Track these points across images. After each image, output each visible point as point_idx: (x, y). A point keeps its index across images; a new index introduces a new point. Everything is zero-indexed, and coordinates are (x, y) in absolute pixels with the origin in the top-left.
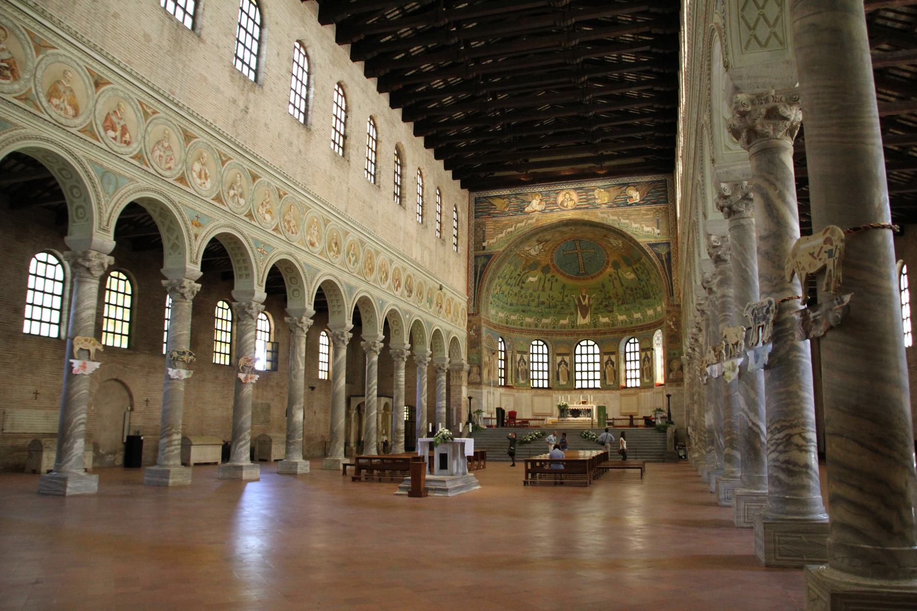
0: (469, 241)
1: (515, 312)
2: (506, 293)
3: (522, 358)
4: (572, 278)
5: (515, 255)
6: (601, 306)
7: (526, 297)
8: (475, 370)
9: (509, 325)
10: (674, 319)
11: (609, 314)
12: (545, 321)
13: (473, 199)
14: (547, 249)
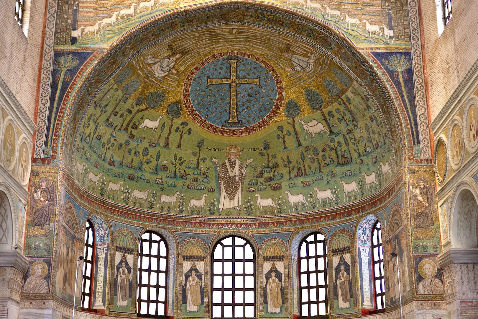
0: (44, 27)
1: (118, 176)
2: (104, 140)
3: (124, 261)
4: (215, 130)
5: (127, 67)
6: (261, 180)
7: (137, 154)
8: (39, 269)
9: (105, 198)
10: (422, 184)
11: (276, 193)
12: (165, 199)
14: (182, 69)
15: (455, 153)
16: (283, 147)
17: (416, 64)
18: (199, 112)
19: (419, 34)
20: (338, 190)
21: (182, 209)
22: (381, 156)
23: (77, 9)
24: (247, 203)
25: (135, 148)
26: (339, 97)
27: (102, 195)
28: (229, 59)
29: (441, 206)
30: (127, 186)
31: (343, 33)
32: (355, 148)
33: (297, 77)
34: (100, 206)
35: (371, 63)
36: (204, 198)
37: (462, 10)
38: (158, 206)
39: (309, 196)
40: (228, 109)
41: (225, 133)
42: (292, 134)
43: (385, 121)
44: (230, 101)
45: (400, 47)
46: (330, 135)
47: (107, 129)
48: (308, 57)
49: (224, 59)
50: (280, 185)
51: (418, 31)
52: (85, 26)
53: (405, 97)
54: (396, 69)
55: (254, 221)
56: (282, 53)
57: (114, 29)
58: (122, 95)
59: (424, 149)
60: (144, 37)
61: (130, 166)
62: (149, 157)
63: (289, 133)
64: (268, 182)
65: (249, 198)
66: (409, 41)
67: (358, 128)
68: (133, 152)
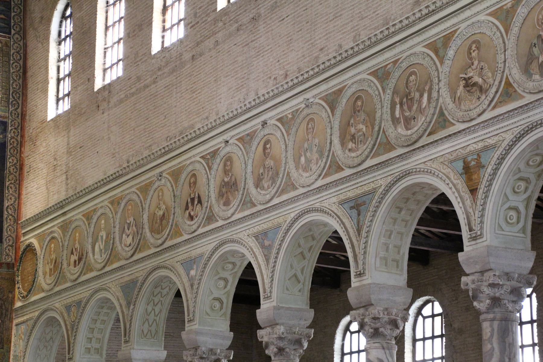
15: (48, 270)
17: (12, 138)
29: (17, 325)
37: (83, 111)
51: (19, 94)
59: (7, 250)
66: (6, 107)
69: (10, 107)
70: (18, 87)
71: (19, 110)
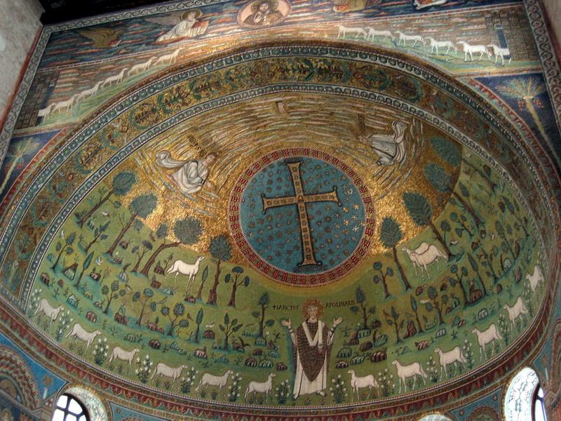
1: (131, 341)
2: (108, 282)
4: (284, 278)
6: (356, 348)
7: (165, 311)
9: (102, 369)
11: (378, 366)
12: (209, 379)
13: (46, 35)
16: (384, 294)
18: (258, 251)
19: (552, 48)
20: (471, 345)
21: (236, 394)
22: (526, 264)
23: (53, 88)
24: (336, 384)
25: (160, 303)
26: (452, 191)
27: (98, 362)
28: (287, 162)
30: (147, 357)
31: (428, 59)
32: (488, 268)
33: (387, 176)
34: (93, 379)
35: (478, 93)
36: (270, 379)
38: (196, 390)
39: (428, 363)
40: (299, 245)
41: (299, 282)
42: (396, 272)
43: (519, 195)
44: (301, 232)
45: (523, 67)
46: (449, 260)
47: (111, 266)
48: (391, 132)
49: (280, 164)
50: (385, 351)
52: (57, 102)
53: (543, 132)
54: (520, 97)
55: (346, 411)
56: (357, 136)
57: (93, 99)
58: (130, 216)
60: (140, 112)
61: (154, 327)
62: (185, 316)
63: (390, 272)
64: (366, 350)
65: (339, 376)
67: (487, 235)
68: (159, 307)
69: (542, 58)
70: (545, 39)
71: (554, 59)
